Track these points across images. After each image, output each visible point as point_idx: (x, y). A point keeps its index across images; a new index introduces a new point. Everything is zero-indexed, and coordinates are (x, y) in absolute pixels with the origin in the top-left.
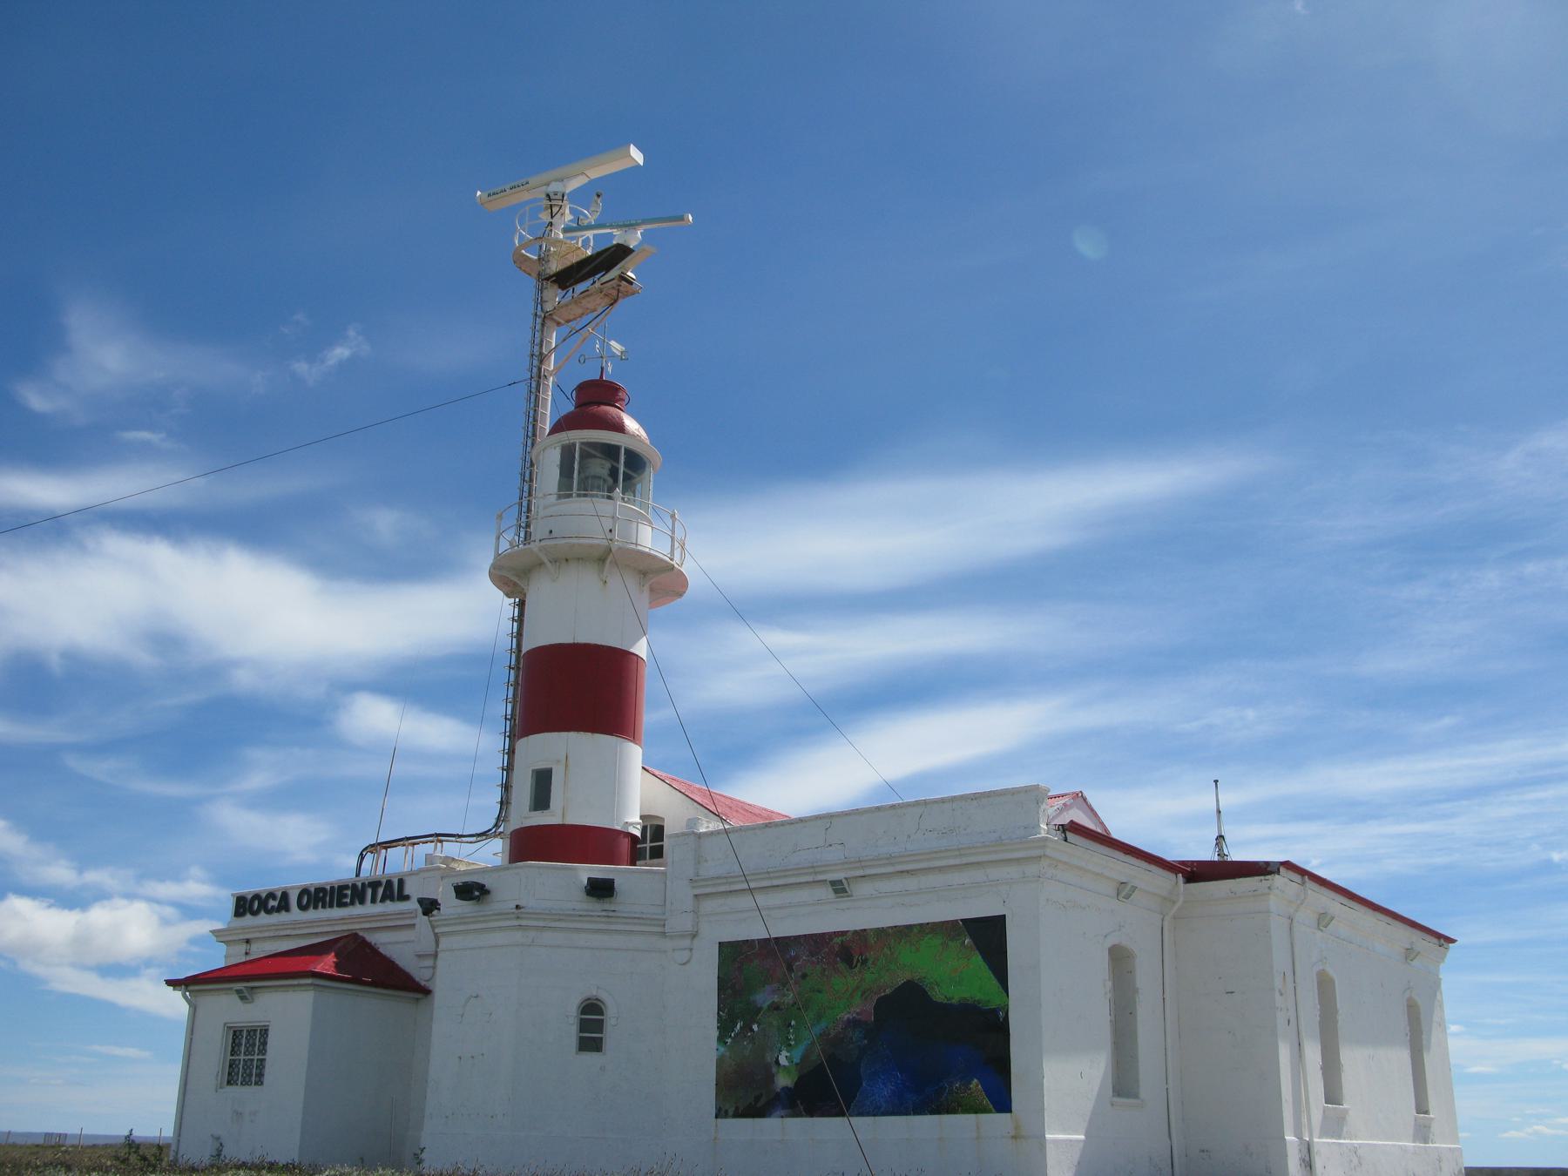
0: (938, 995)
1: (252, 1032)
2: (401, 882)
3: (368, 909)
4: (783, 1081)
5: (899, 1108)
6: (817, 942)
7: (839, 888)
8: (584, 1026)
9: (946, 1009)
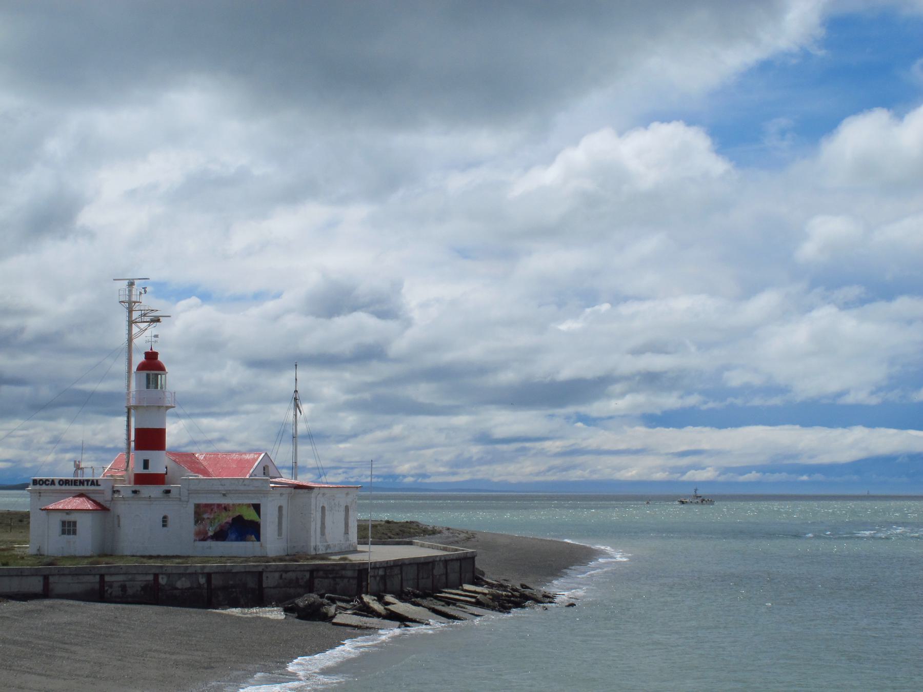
0: (246, 518)
4: (211, 534)
5: (237, 540)
6: (219, 505)
7: (224, 495)
8: (164, 521)
9: (247, 521)
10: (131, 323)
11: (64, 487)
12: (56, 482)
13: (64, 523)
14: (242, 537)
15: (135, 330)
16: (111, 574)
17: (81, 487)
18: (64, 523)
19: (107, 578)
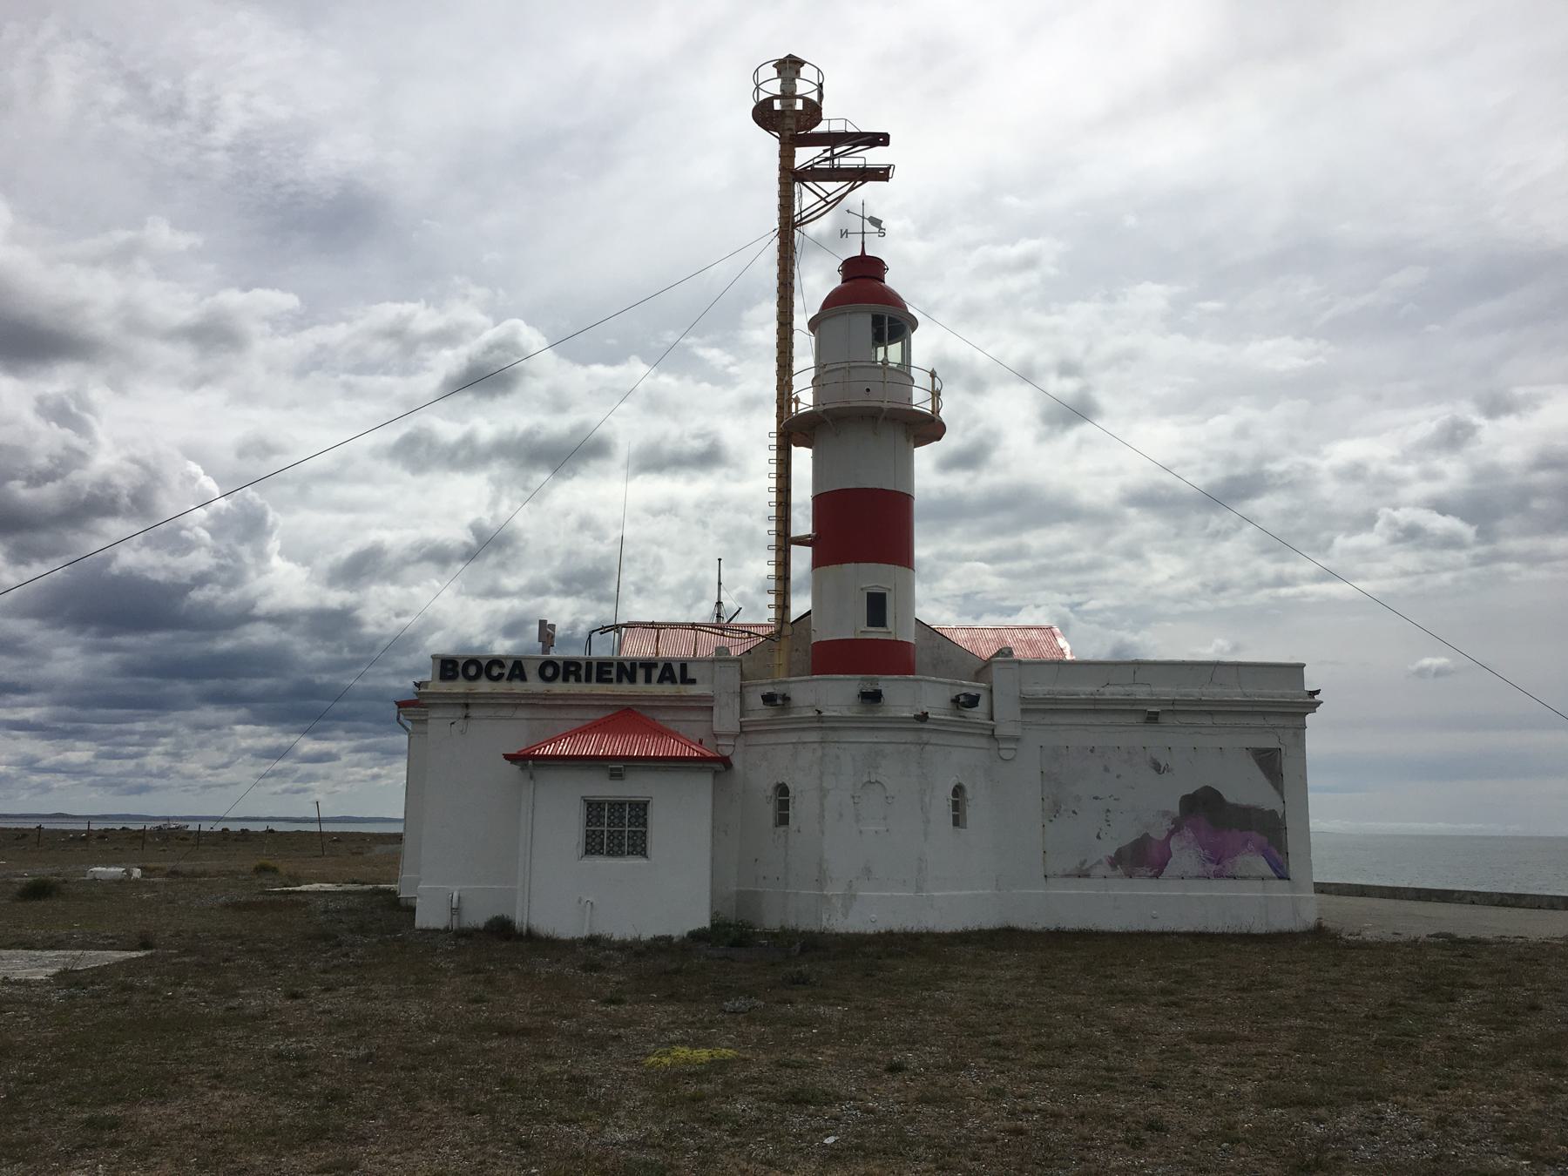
0: (1230, 798)
1: (638, 804)
2: (684, 666)
3: (640, 687)
9: (1236, 807)
10: (791, 176)
11: (558, 687)
12: (532, 671)
14: (1218, 865)
15: (806, 198)
17: (625, 688)
18: (594, 809)
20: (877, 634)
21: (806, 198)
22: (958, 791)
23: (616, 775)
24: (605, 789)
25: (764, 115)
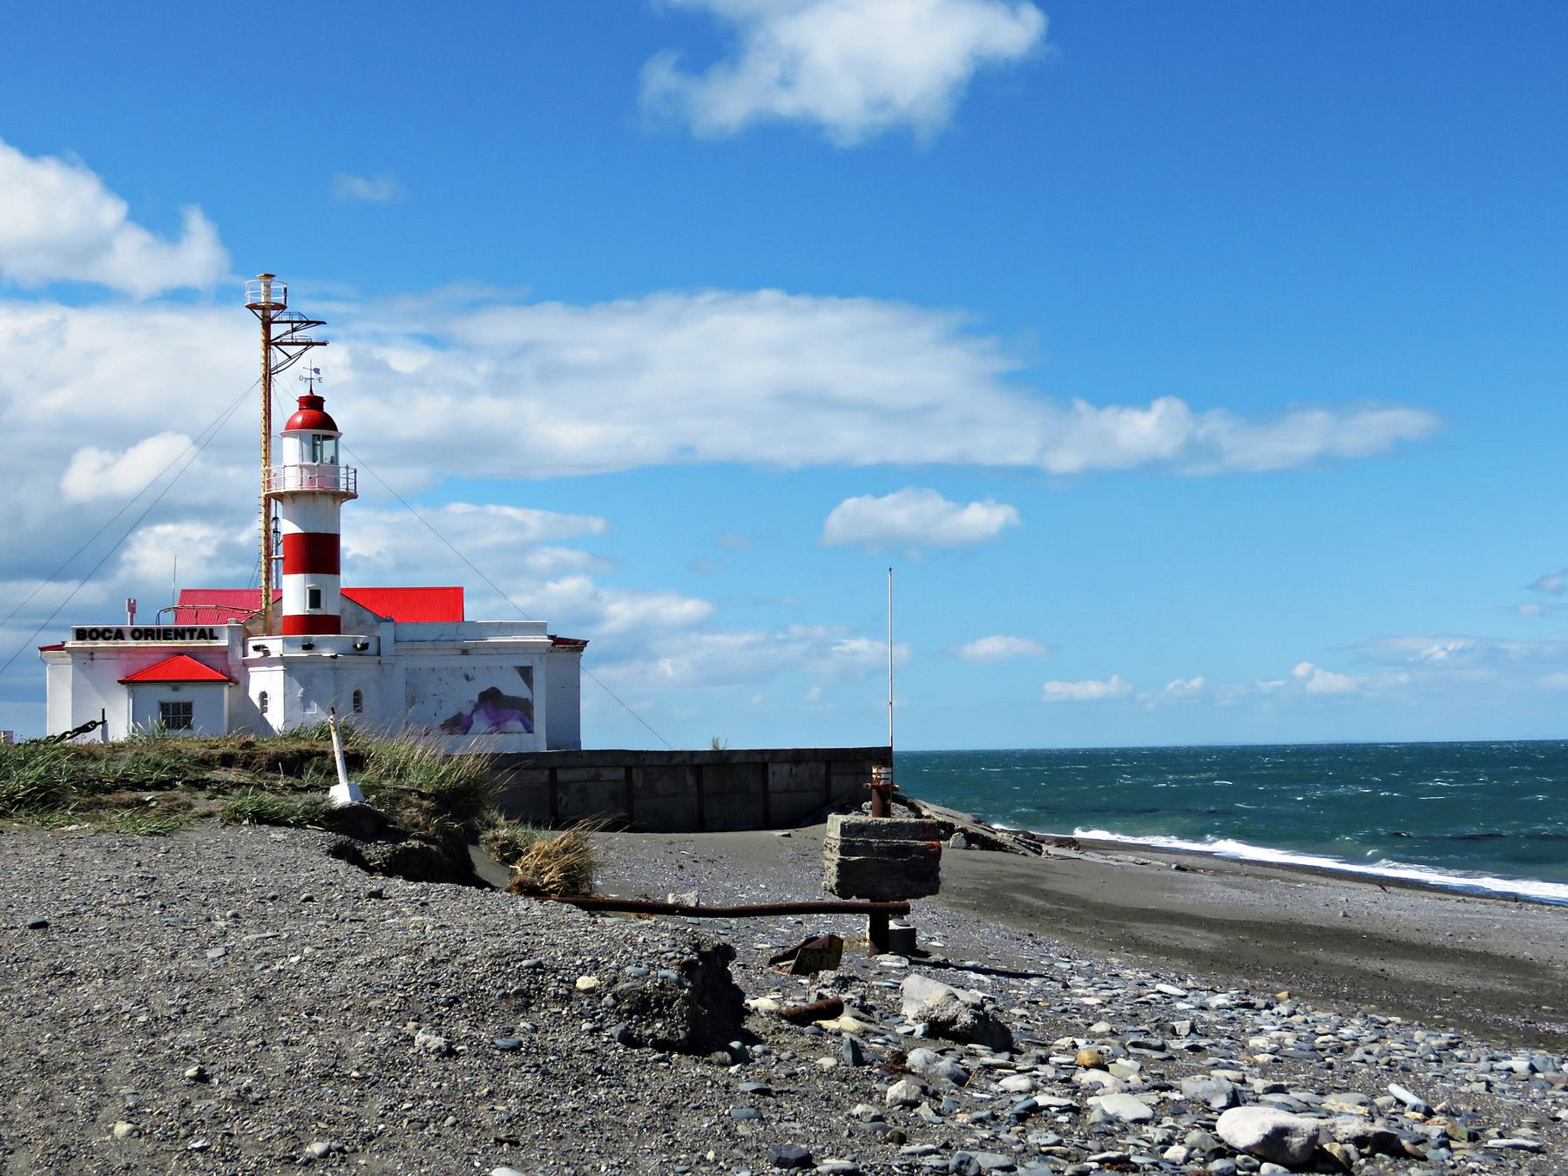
0: (505, 693)
10: (268, 343)
11: (142, 643)
12: (127, 635)
13: (164, 707)
16: (566, 768)
18: (164, 707)
19: (562, 776)
20: (317, 612)
21: (277, 356)
22: (357, 694)
23: (175, 689)
24: (167, 695)
25: (252, 307)
